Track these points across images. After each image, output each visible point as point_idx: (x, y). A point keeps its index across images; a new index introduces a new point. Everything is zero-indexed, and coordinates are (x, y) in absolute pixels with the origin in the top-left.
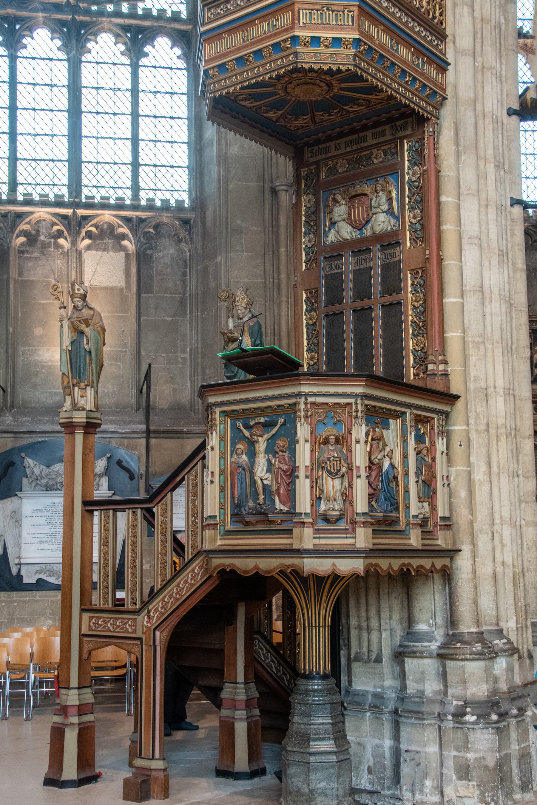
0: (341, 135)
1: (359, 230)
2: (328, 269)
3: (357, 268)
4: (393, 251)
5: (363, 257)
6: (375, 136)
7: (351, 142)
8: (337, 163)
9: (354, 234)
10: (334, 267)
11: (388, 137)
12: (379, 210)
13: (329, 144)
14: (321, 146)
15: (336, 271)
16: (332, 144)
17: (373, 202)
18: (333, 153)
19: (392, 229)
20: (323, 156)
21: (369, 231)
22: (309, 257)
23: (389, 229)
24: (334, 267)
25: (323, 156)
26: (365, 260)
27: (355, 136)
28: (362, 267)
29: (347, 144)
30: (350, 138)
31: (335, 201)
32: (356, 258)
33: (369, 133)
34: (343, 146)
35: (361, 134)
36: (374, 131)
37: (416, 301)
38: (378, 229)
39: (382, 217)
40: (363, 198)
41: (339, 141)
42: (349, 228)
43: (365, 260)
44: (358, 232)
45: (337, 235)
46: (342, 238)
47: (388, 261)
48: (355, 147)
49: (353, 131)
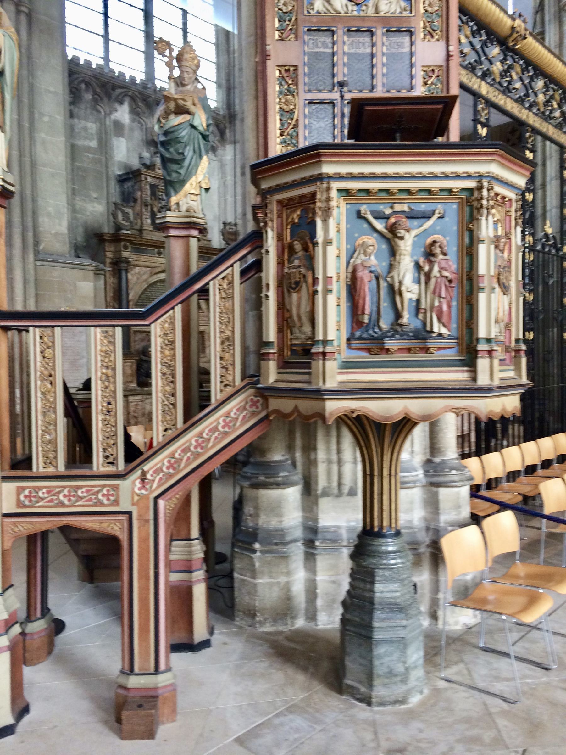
1: (357, 4)
2: (311, 45)
3: (353, 51)
5: (361, 39)
9: (350, 8)
10: (320, 45)
15: (322, 50)
19: (401, 13)
21: (370, 9)
22: (285, 24)
23: (398, 11)
24: (320, 45)
26: (364, 44)
28: (359, 51)
32: (351, 39)
43: (364, 44)
44: (355, 8)
45: (326, 4)
46: (335, 10)
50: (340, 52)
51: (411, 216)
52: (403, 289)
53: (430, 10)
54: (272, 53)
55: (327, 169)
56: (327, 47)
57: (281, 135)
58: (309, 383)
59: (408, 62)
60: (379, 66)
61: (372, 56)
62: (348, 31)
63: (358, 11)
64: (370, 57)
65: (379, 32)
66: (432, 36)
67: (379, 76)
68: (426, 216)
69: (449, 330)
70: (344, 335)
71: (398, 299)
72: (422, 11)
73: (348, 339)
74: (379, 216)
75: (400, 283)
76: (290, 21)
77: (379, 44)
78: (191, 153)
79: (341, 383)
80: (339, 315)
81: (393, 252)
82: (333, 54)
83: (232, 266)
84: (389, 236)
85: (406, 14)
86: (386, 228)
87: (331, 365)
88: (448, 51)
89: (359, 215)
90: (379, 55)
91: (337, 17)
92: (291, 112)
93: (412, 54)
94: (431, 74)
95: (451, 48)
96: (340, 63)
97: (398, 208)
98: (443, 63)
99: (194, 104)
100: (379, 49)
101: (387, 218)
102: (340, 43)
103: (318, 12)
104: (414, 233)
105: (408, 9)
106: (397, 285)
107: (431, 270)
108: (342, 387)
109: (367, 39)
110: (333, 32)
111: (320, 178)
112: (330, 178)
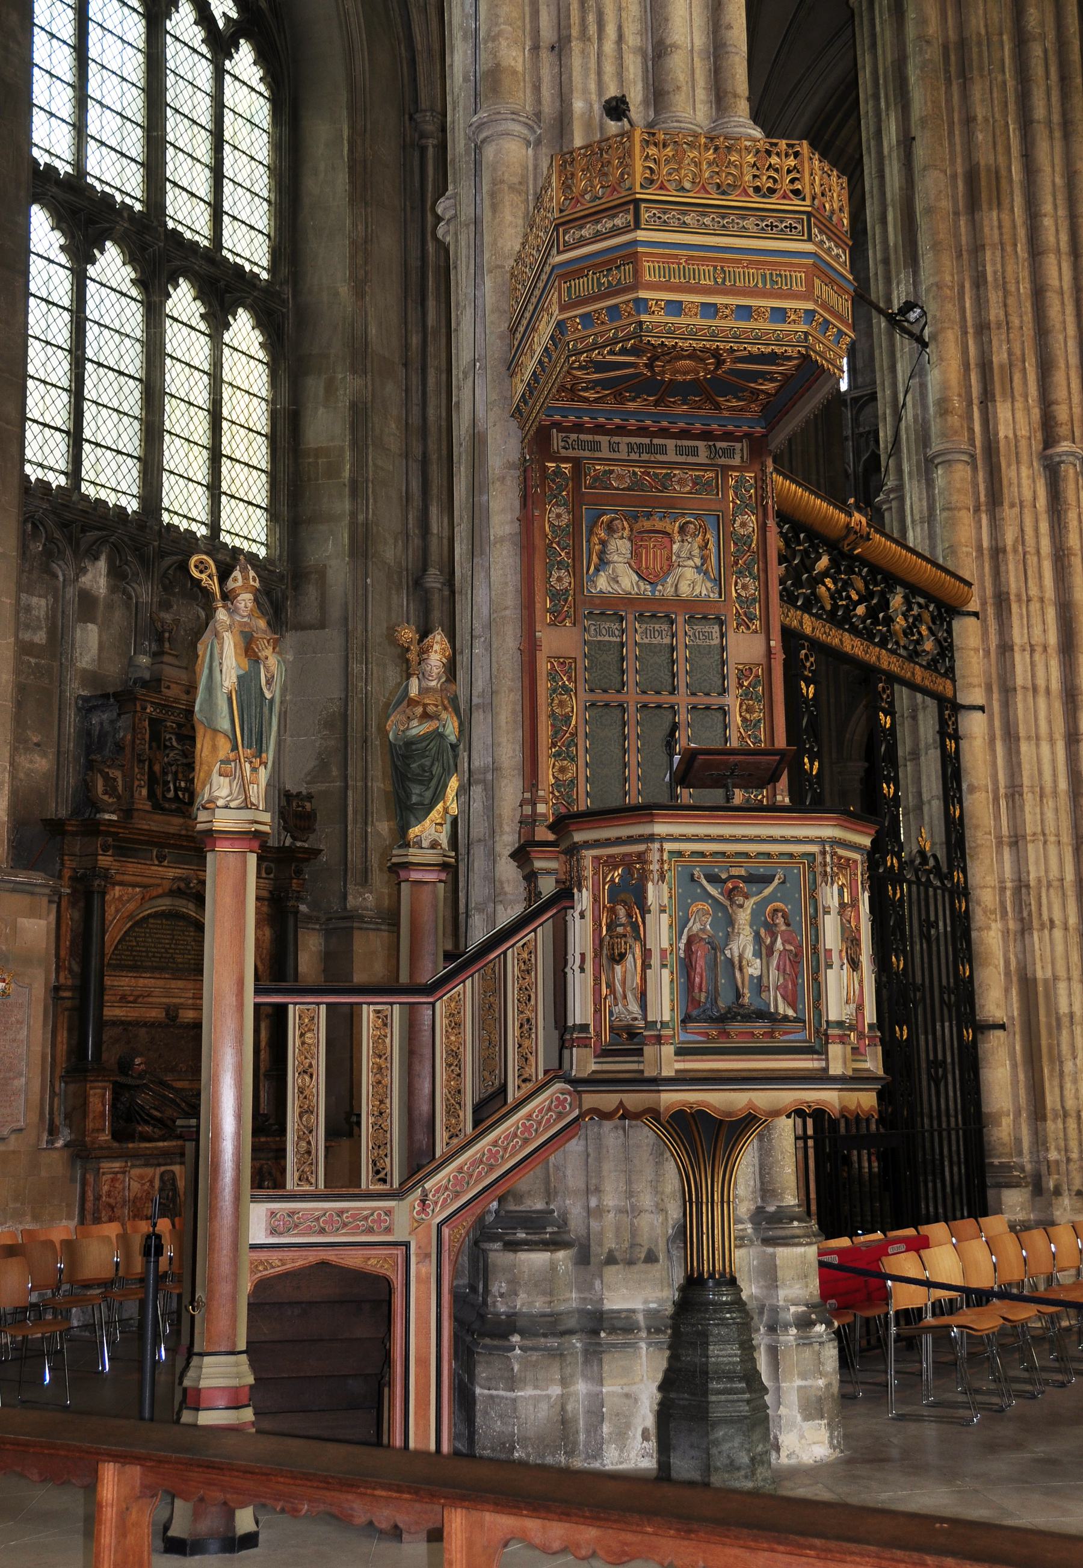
0: (621, 430)
3: (646, 641)
4: (707, 629)
5: (657, 627)
6: (679, 450)
7: (638, 448)
8: (611, 472)
11: (702, 458)
12: (691, 563)
13: (597, 438)
14: (582, 437)
15: (607, 638)
16: (604, 440)
17: (675, 547)
18: (605, 453)
20: (587, 454)
25: (587, 454)
26: (660, 633)
27: (647, 441)
29: (631, 447)
30: (639, 440)
31: (610, 529)
32: (644, 626)
33: (670, 443)
34: (623, 448)
35: (656, 441)
36: (679, 442)
37: (747, 711)
38: (685, 590)
39: (690, 573)
40: (666, 540)
41: (616, 439)
42: (635, 578)
43: (660, 633)
47: (700, 643)
48: (645, 457)
49: (642, 431)
50: (631, 642)
51: (750, 879)
52: (744, 963)
53: (743, 594)
54: (544, 644)
55: (660, 829)
56: (614, 635)
57: (554, 745)
58: (642, 1072)
59: (717, 657)
60: (682, 661)
61: (673, 649)
62: (641, 615)
63: (653, 592)
64: (668, 650)
65: (680, 620)
66: (748, 628)
67: (682, 674)
68: (767, 880)
69: (795, 1011)
70: (678, 1018)
71: (738, 974)
72: (734, 594)
73: (683, 1021)
74: (713, 879)
75: (741, 957)
76: (566, 600)
77: (681, 634)
78: (440, 770)
79: (677, 1071)
80: (672, 993)
81: (731, 922)
82: (622, 645)
83: (535, 930)
84: (727, 903)
85: (714, 596)
86: (721, 894)
87: (668, 1050)
88: (769, 647)
89: (692, 878)
90: (681, 647)
91: (628, 601)
92: (567, 719)
93: (723, 649)
94: (747, 673)
95: (773, 643)
96: (631, 656)
97: (735, 871)
98: (764, 661)
99: (445, 708)
100: (681, 641)
101: (725, 882)
102: (630, 631)
103: (601, 592)
104: (753, 900)
105: (717, 590)
106: (736, 960)
107: (774, 942)
108: (681, 1075)
109: (665, 627)
110: (622, 619)
111: (651, 838)
112: (663, 839)
